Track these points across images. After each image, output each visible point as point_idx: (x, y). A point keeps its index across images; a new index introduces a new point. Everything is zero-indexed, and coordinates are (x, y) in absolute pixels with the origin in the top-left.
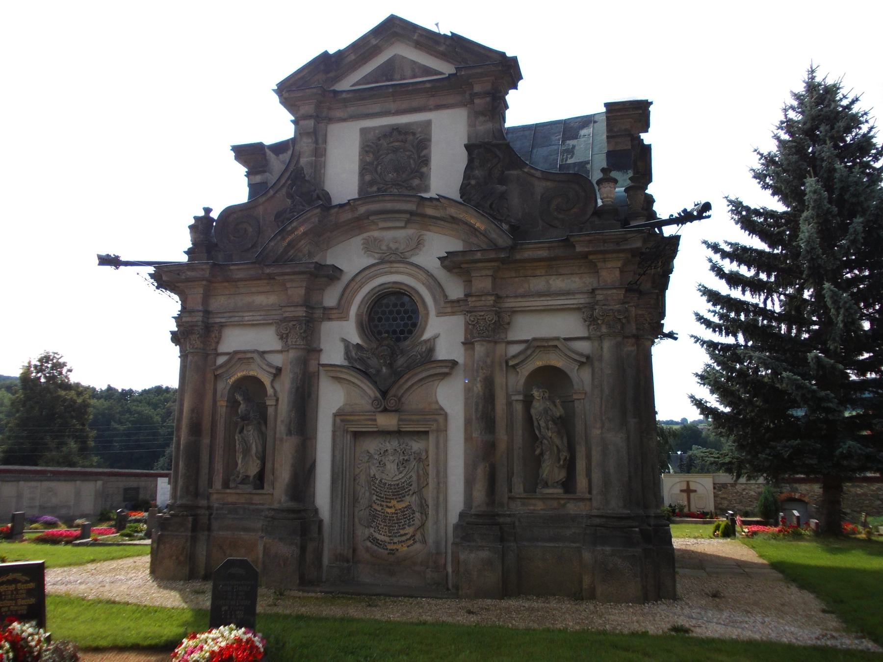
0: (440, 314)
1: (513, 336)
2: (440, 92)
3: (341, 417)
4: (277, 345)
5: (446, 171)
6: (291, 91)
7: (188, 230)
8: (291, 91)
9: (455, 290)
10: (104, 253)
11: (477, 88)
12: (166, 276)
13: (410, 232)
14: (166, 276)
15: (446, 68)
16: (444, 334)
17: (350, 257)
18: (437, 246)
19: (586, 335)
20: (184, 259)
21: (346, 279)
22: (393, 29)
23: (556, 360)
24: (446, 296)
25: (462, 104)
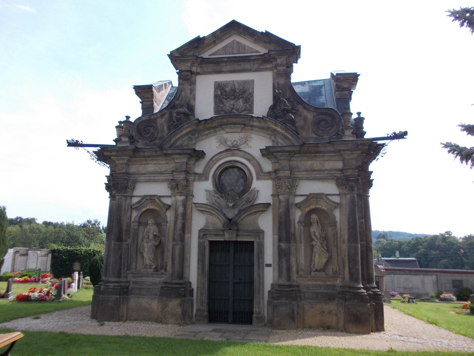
0: (258, 179)
1: (298, 193)
2: (262, 62)
3: (203, 233)
4: (168, 193)
5: (262, 103)
6: (177, 57)
7: (115, 129)
8: (177, 57)
9: (267, 166)
10: (70, 139)
11: (279, 61)
12: (103, 154)
13: (242, 135)
14: (103, 154)
15: (262, 50)
16: (263, 190)
17: (210, 146)
18: (256, 143)
19: (338, 193)
20: (114, 143)
21: (207, 158)
22: (234, 27)
23: (322, 206)
24: (262, 170)
25: (271, 69)
